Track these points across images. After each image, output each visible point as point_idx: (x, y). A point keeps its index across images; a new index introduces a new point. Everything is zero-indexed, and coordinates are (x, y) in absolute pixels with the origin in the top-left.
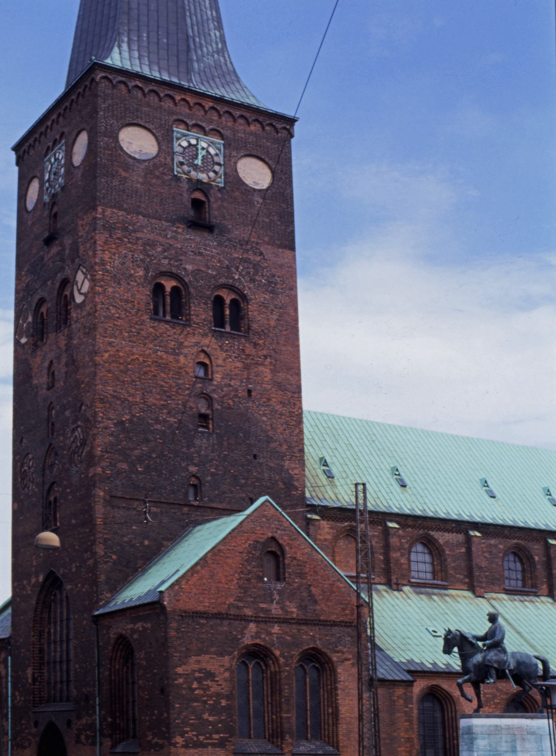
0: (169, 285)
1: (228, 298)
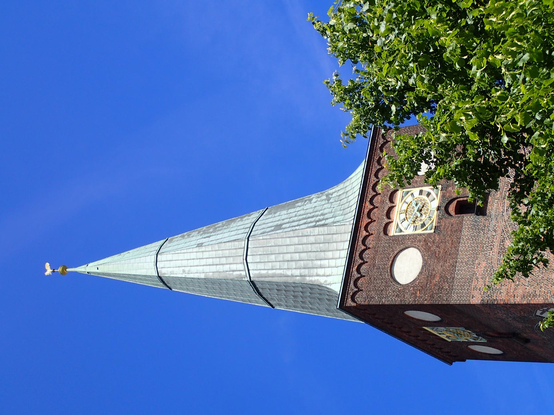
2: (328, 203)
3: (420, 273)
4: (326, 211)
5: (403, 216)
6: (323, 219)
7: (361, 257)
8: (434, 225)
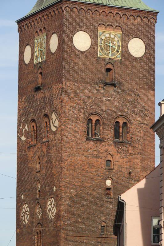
0: (94, 118)
1: (121, 121)
3: (78, 50)
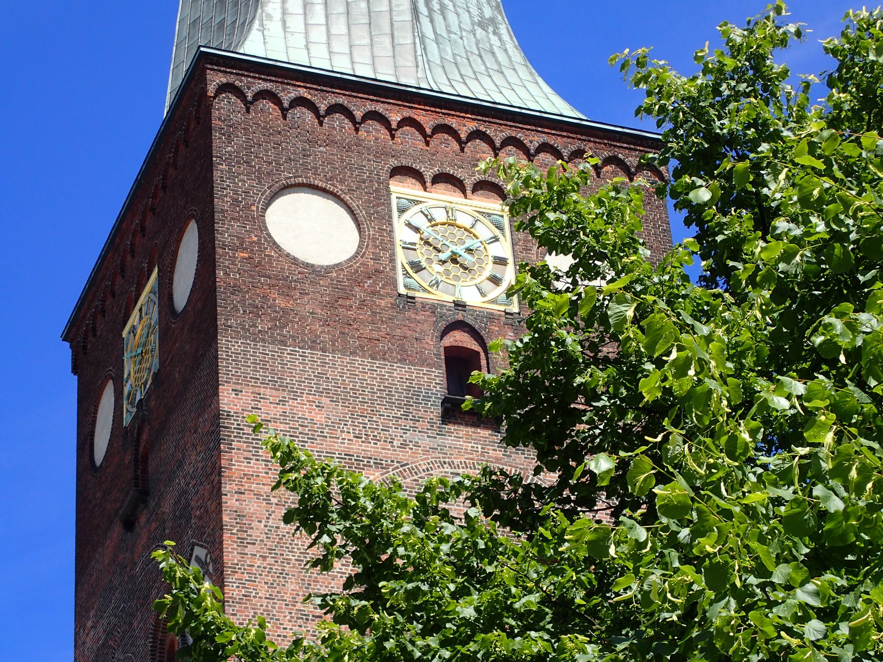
2: (473, 24)
3: (295, 259)
4: (452, 17)
5: (440, 216)
6: (430, 10)
7: (334, 109)
8: (417, 294)
